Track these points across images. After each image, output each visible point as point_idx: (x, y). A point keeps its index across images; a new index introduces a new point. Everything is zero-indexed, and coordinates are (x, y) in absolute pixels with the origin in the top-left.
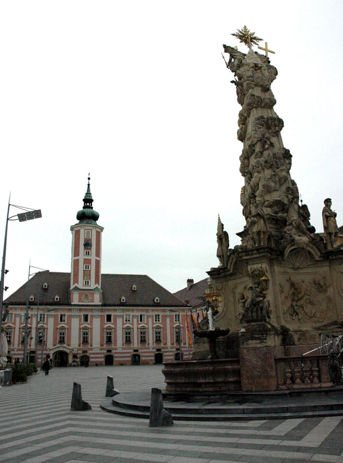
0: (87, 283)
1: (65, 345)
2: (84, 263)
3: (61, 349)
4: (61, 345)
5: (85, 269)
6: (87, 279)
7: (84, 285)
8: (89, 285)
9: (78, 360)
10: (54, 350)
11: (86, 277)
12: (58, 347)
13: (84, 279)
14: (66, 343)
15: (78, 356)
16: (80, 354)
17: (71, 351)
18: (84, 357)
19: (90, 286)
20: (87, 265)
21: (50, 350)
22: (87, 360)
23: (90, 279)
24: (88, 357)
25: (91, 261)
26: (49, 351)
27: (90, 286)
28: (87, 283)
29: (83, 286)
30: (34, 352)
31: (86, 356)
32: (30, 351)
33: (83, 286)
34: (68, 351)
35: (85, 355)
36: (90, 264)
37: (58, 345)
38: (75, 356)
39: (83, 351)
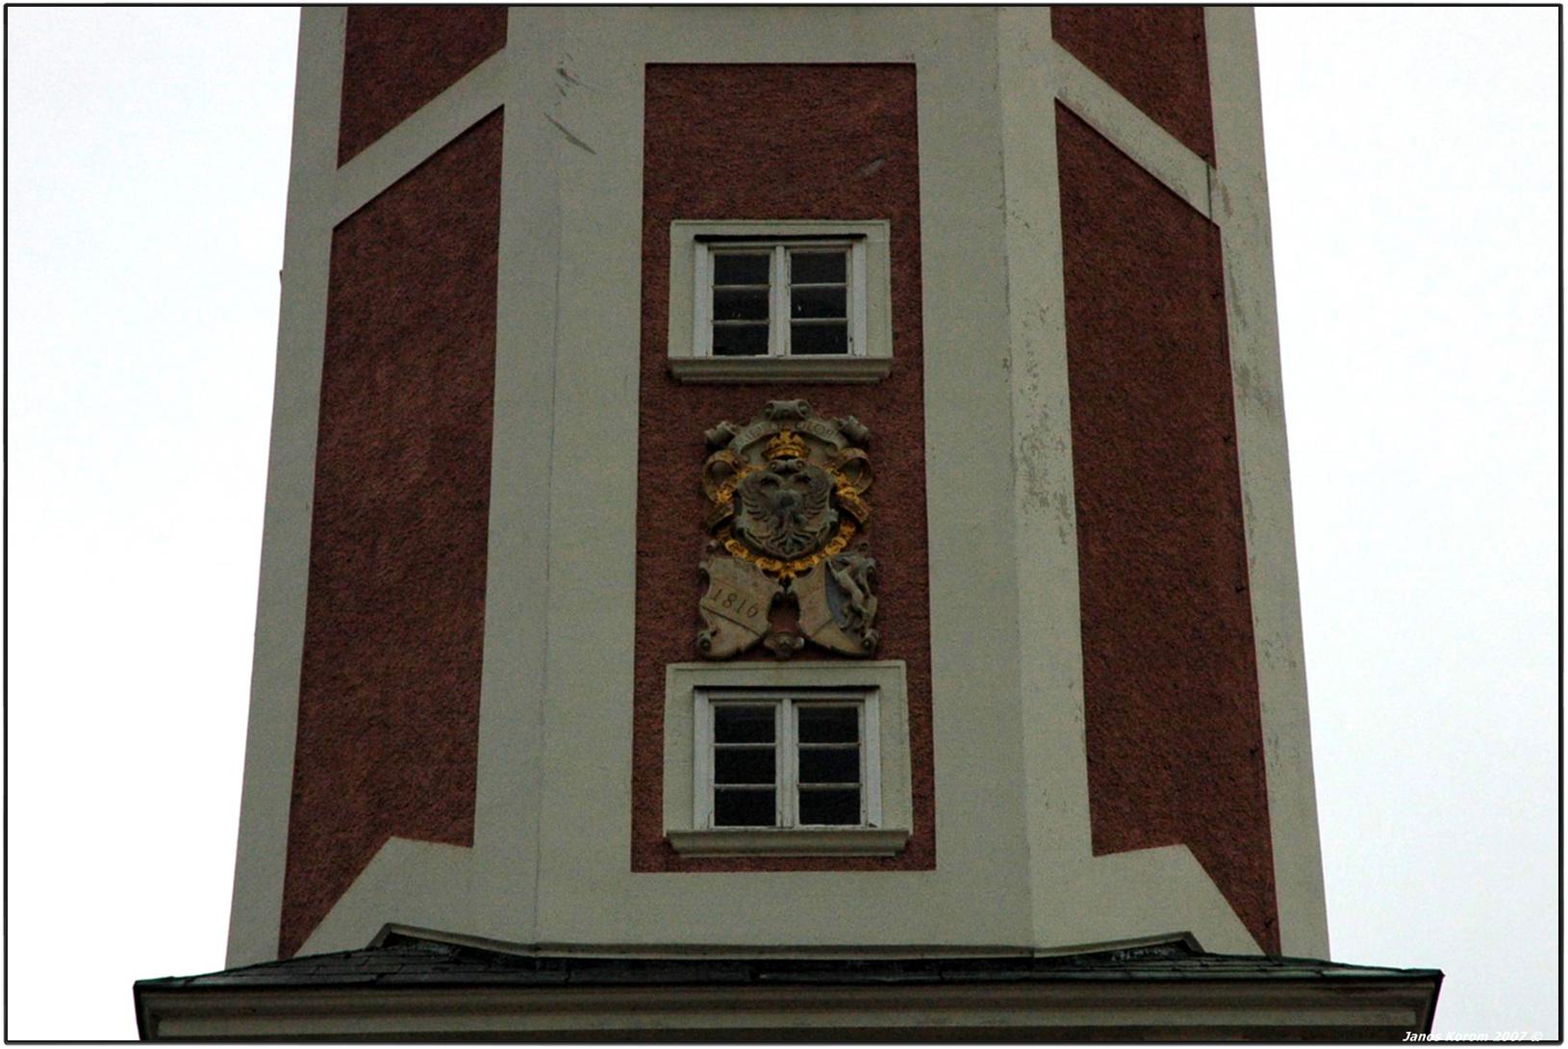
0: (791, 782)
2: (670, 190)
5: (693, 337)
6: (782, 638)
7: (691, 802)
8: (883, 805)
11: (737, 590)
13: (668, 629)
19: (915, 852)
20: (781, 242)
23: (895, 618)
25: (905, 126)
27: (915, 852)
28: (788, 782)
29: (655, 852)
33: (655, 852)
36: (898, 201)
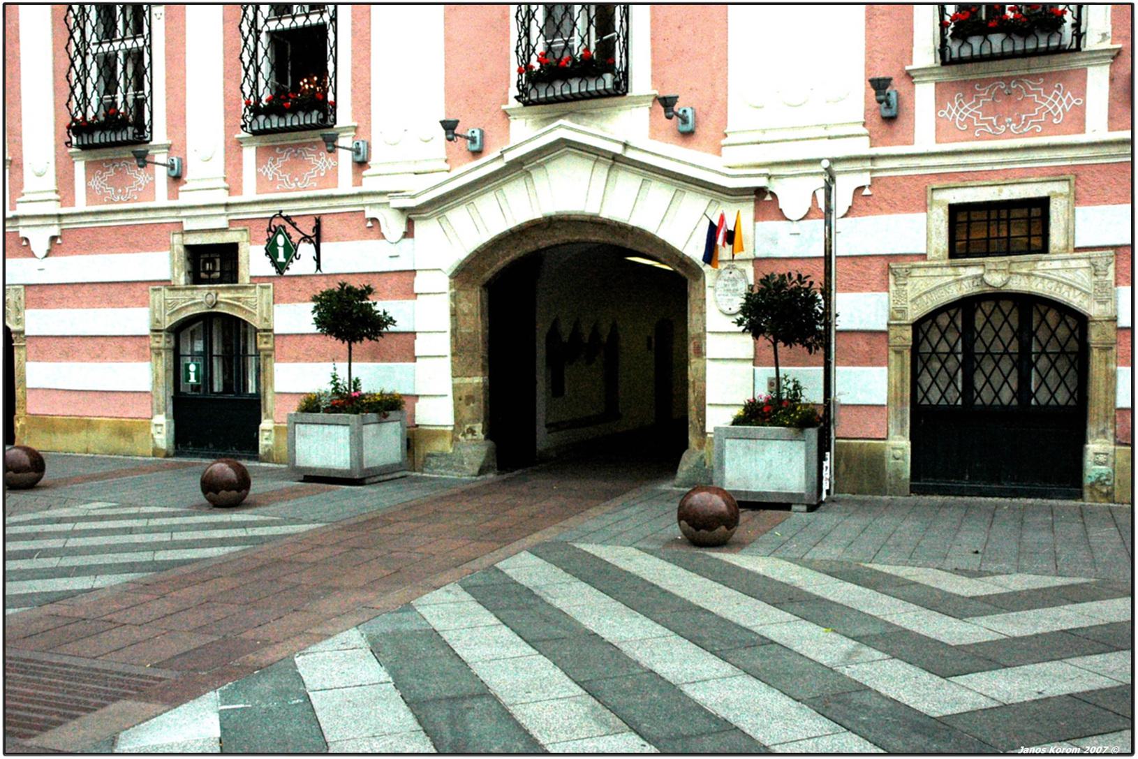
1: (627, 125)
3: (568, 191)
4: (565, 128)
9: (867, 386)
10: (458, 215)
12: (520, 167)
14: (641, 83)
15: (856, 310)
16: (889, 268)
17: (740, 215)
18: (998, 334)
21: (411, 216)
22: (1048, 391)
24: (1081, 321)
26: (393, 225)
30: (212, 262)
31: (1028, 303)
32: (178, 241)
34: (679, 225)
35: (998, 297)
37: (526, 132)
38: (788, 313)
39: (955, 210)
